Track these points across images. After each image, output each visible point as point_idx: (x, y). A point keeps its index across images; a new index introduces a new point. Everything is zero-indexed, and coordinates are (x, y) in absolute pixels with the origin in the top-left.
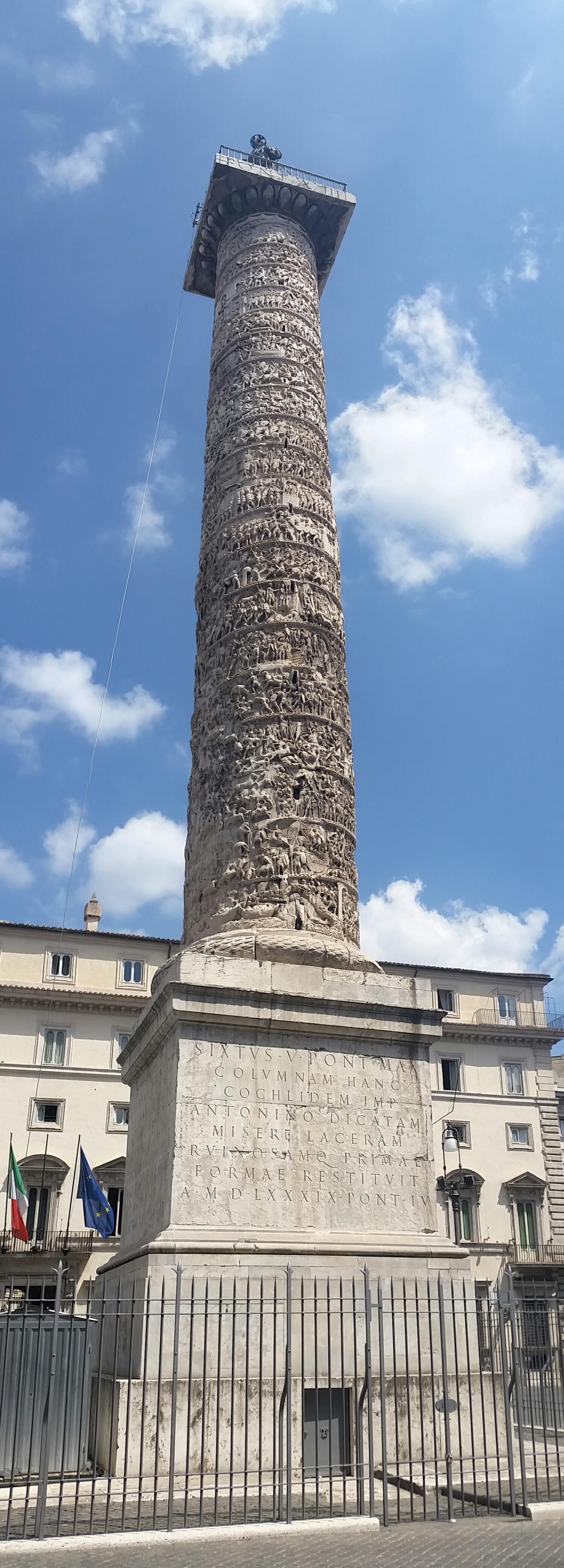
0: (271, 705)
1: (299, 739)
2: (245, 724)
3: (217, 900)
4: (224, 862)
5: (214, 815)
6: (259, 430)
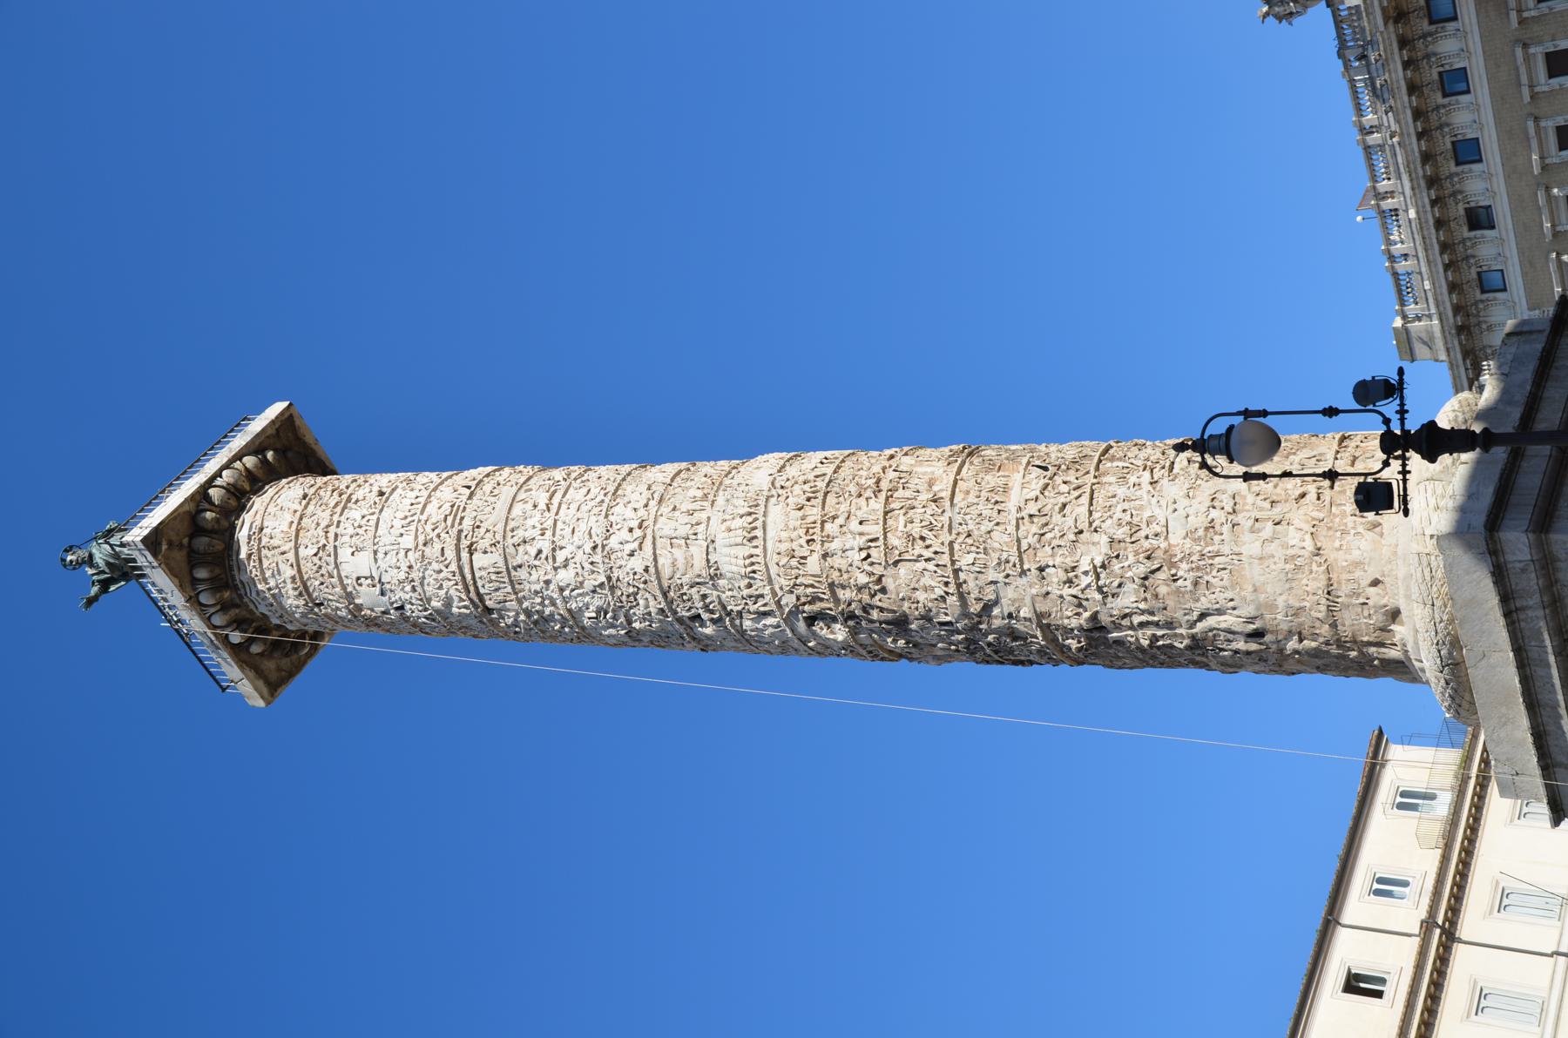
0: (1072, 492)
1: (1132, 464)
2: (1091, 524)
3: (1345, 564)
4: (1291, 552)
5: (1214, 573)
6: (629, 513)
